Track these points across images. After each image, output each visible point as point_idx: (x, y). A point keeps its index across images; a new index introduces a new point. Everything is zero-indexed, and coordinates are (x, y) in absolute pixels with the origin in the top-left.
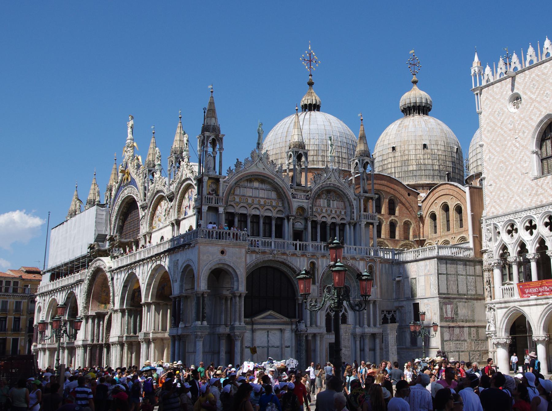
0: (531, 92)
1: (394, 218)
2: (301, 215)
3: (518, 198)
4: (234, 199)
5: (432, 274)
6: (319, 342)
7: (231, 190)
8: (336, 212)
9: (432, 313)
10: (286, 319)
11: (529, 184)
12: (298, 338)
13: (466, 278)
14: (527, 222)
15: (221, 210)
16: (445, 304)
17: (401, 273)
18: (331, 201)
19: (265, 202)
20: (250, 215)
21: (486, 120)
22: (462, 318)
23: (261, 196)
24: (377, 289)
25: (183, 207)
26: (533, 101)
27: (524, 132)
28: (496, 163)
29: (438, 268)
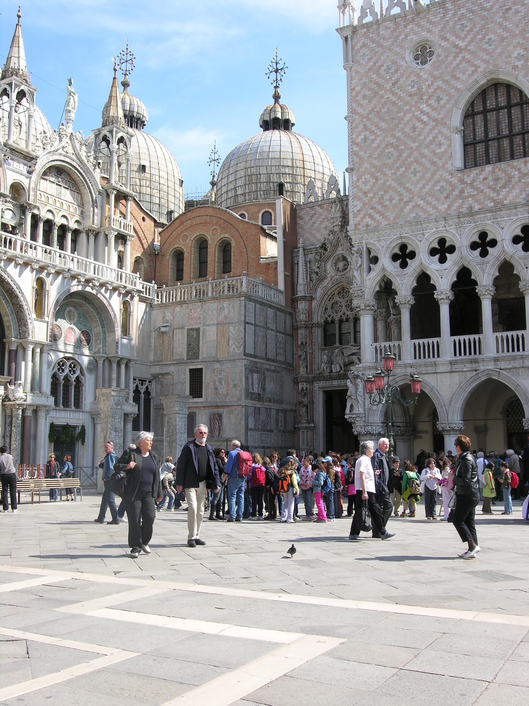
0: (457, 37)
3: (421, 202)
5: (232, 323)
6: (44, 420)
9: (228, 385)
11: (447, 181)
13: (276, 336)
14: (437, 240)
16: (252, 371)
17: (167, 321)
21: (360, 79)
22: (270, 396)
26: (460, 50)
27: (439, 99)
28: (378, 146)
29: (245, 313)
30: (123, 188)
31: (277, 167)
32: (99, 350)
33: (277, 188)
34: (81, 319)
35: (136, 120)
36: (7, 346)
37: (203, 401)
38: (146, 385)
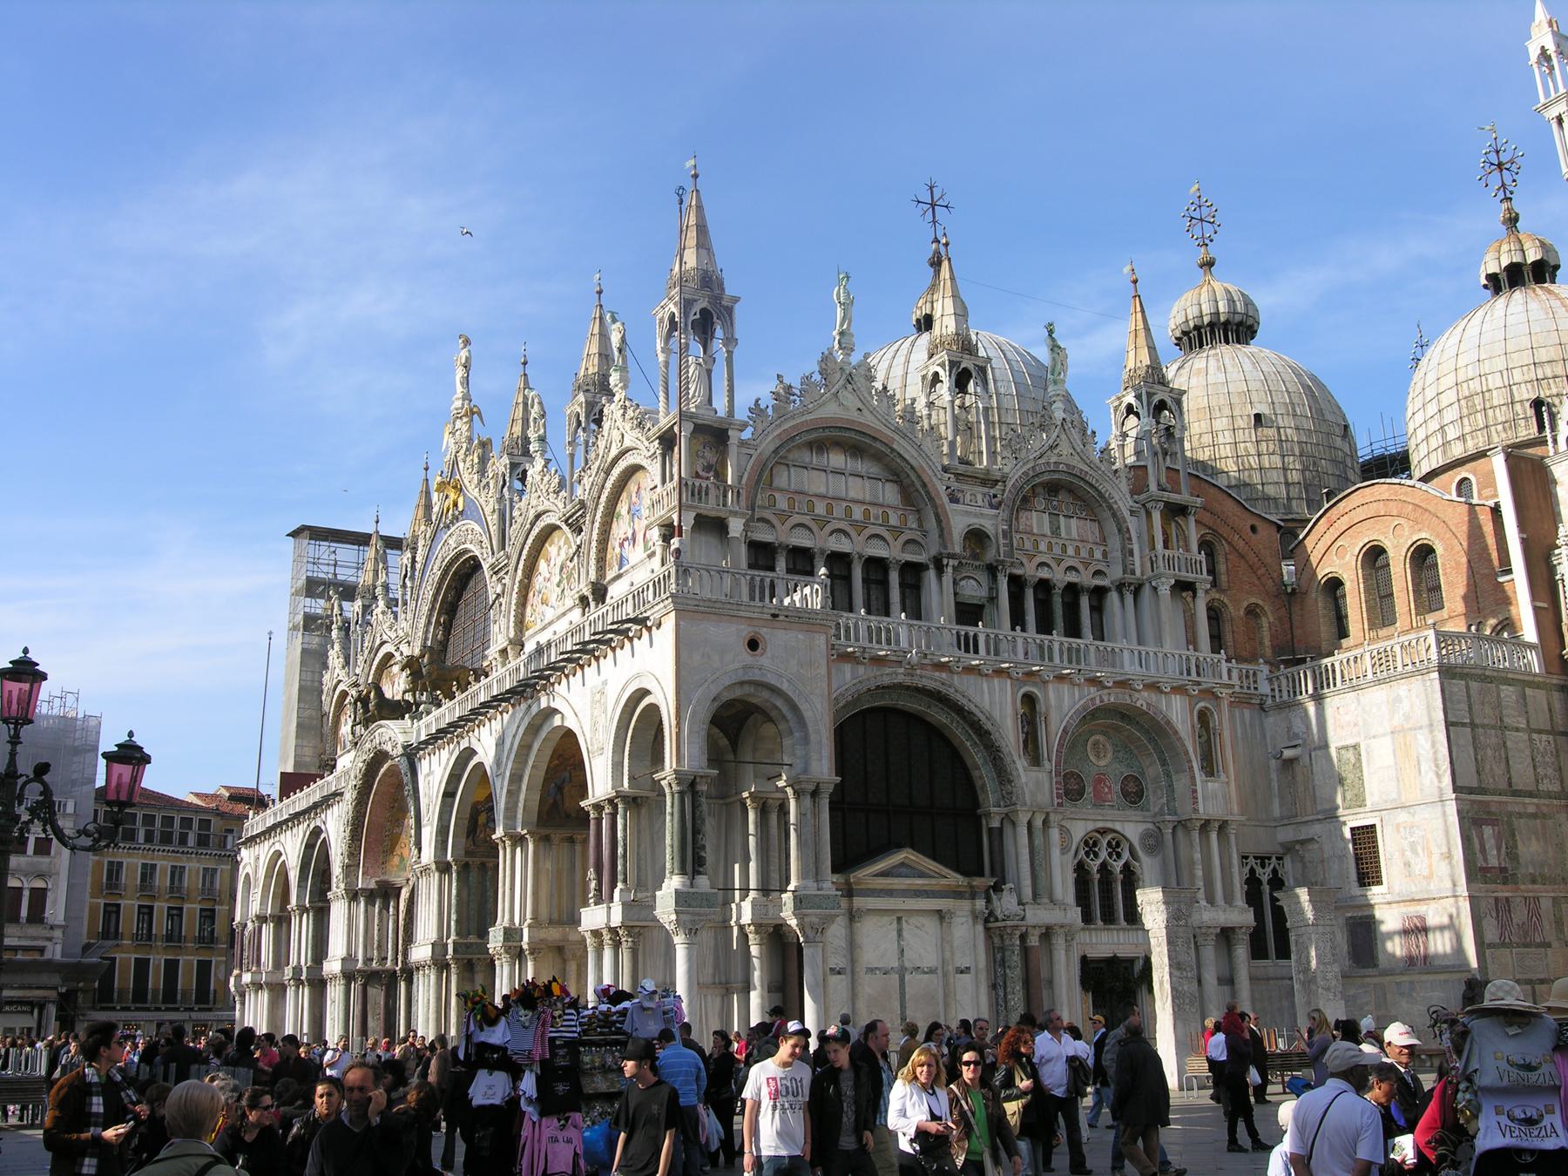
1: (1217, 596)
2: (975, 557)
4: (772, 503)
6: (1063, 952)
7: (760, 475)
8: (1077, 550)
9: (1430, 854)
10: (955, 879)
12: (997, 940)
13: (1530, 740)
15: (736, 527)
17: (1296, 736)
18: (1062, 519)
19: (867, 513)
20: (822, 551)
22: (1531, 871)
23: (852, 494)
24: (1227, 783)
25: (614, 543)
30: (1174, 497)
31: (1525, 368)
32: (1162, 809)
33: (1531, 412)
34: (1121, 755)
35: (1235, 328)
36: (984, 822)
37: (1384, 892)
38: (1272, 867)
